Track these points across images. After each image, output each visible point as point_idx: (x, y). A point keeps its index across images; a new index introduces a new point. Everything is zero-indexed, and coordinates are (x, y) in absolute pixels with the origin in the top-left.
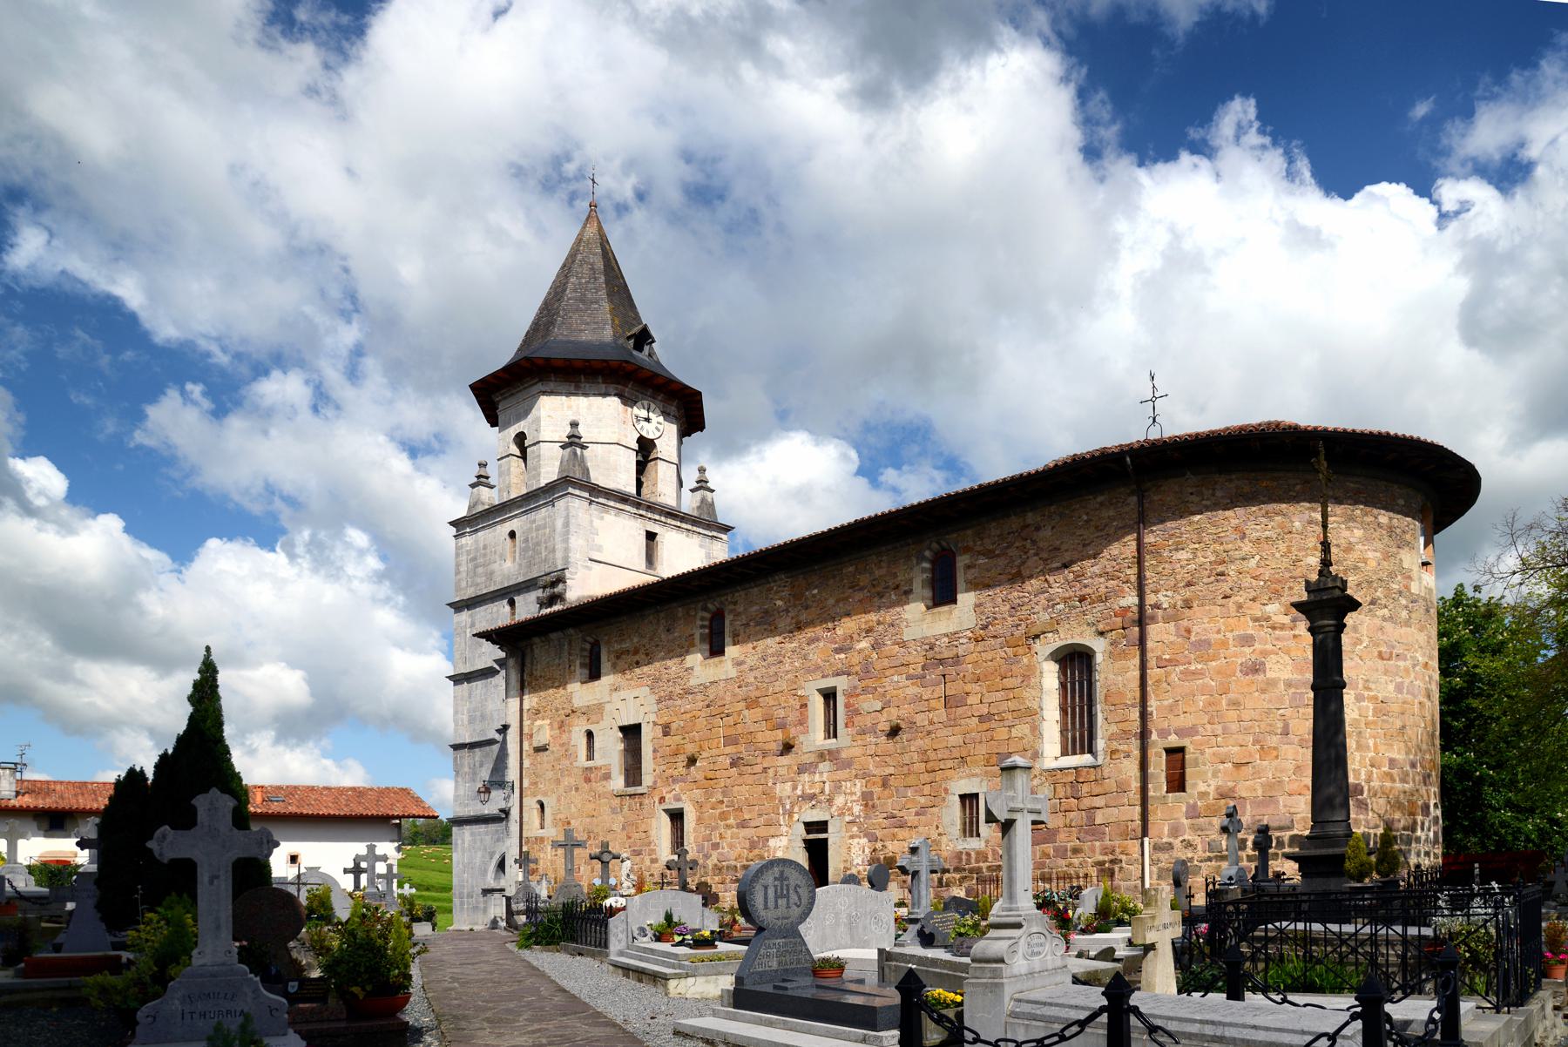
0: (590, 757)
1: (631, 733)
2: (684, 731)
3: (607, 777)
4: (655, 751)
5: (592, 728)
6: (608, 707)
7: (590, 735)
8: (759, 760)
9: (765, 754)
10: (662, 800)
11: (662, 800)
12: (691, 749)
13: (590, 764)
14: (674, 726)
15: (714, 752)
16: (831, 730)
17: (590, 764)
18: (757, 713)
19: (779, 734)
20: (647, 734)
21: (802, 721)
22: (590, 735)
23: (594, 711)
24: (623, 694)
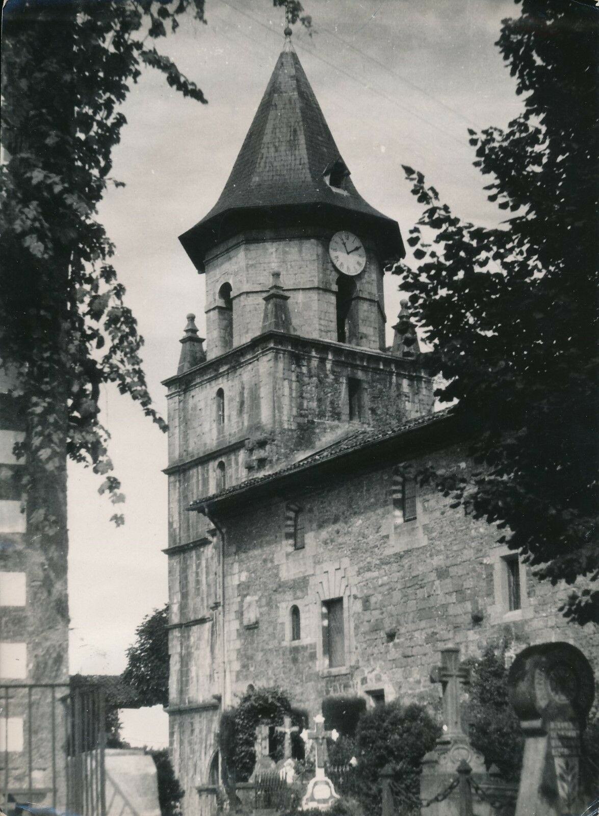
0: (296, 635)
1: (333, 605)
2: (381, 607)
3: (313, 657)
4: (357, 627)
5: (299, 603)
6: (312, 581)
7: (295, 611)
8: (451, 635)
9: (456, 627)
10: (364, 681)
11: (364, 681)
12: (388, 625)
13: (296, 643)
14: (373, 600)
15: (411, 627)
16: (515, 603)
17: (296, 643)
18: (448, 584)
19: (469, 606)
20: (351, 608)
21: (490, 594)
22: (295, 611)
23: (300, 585)
24: (326, 566)
